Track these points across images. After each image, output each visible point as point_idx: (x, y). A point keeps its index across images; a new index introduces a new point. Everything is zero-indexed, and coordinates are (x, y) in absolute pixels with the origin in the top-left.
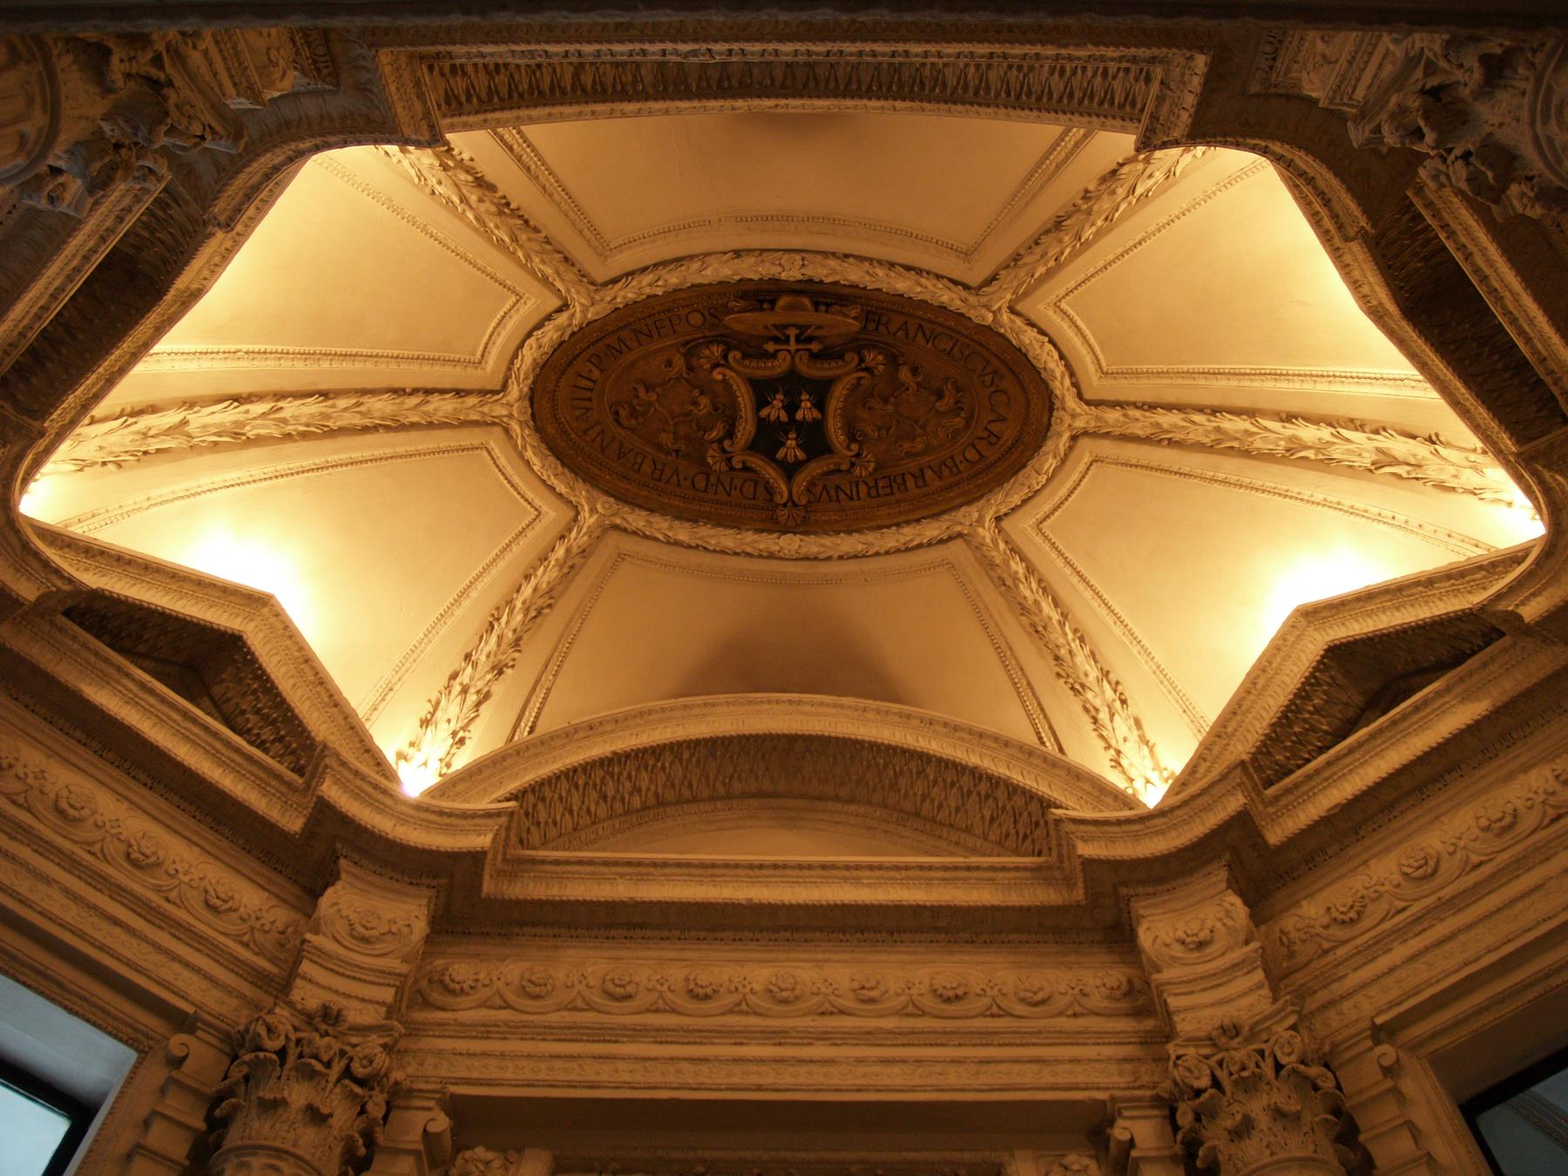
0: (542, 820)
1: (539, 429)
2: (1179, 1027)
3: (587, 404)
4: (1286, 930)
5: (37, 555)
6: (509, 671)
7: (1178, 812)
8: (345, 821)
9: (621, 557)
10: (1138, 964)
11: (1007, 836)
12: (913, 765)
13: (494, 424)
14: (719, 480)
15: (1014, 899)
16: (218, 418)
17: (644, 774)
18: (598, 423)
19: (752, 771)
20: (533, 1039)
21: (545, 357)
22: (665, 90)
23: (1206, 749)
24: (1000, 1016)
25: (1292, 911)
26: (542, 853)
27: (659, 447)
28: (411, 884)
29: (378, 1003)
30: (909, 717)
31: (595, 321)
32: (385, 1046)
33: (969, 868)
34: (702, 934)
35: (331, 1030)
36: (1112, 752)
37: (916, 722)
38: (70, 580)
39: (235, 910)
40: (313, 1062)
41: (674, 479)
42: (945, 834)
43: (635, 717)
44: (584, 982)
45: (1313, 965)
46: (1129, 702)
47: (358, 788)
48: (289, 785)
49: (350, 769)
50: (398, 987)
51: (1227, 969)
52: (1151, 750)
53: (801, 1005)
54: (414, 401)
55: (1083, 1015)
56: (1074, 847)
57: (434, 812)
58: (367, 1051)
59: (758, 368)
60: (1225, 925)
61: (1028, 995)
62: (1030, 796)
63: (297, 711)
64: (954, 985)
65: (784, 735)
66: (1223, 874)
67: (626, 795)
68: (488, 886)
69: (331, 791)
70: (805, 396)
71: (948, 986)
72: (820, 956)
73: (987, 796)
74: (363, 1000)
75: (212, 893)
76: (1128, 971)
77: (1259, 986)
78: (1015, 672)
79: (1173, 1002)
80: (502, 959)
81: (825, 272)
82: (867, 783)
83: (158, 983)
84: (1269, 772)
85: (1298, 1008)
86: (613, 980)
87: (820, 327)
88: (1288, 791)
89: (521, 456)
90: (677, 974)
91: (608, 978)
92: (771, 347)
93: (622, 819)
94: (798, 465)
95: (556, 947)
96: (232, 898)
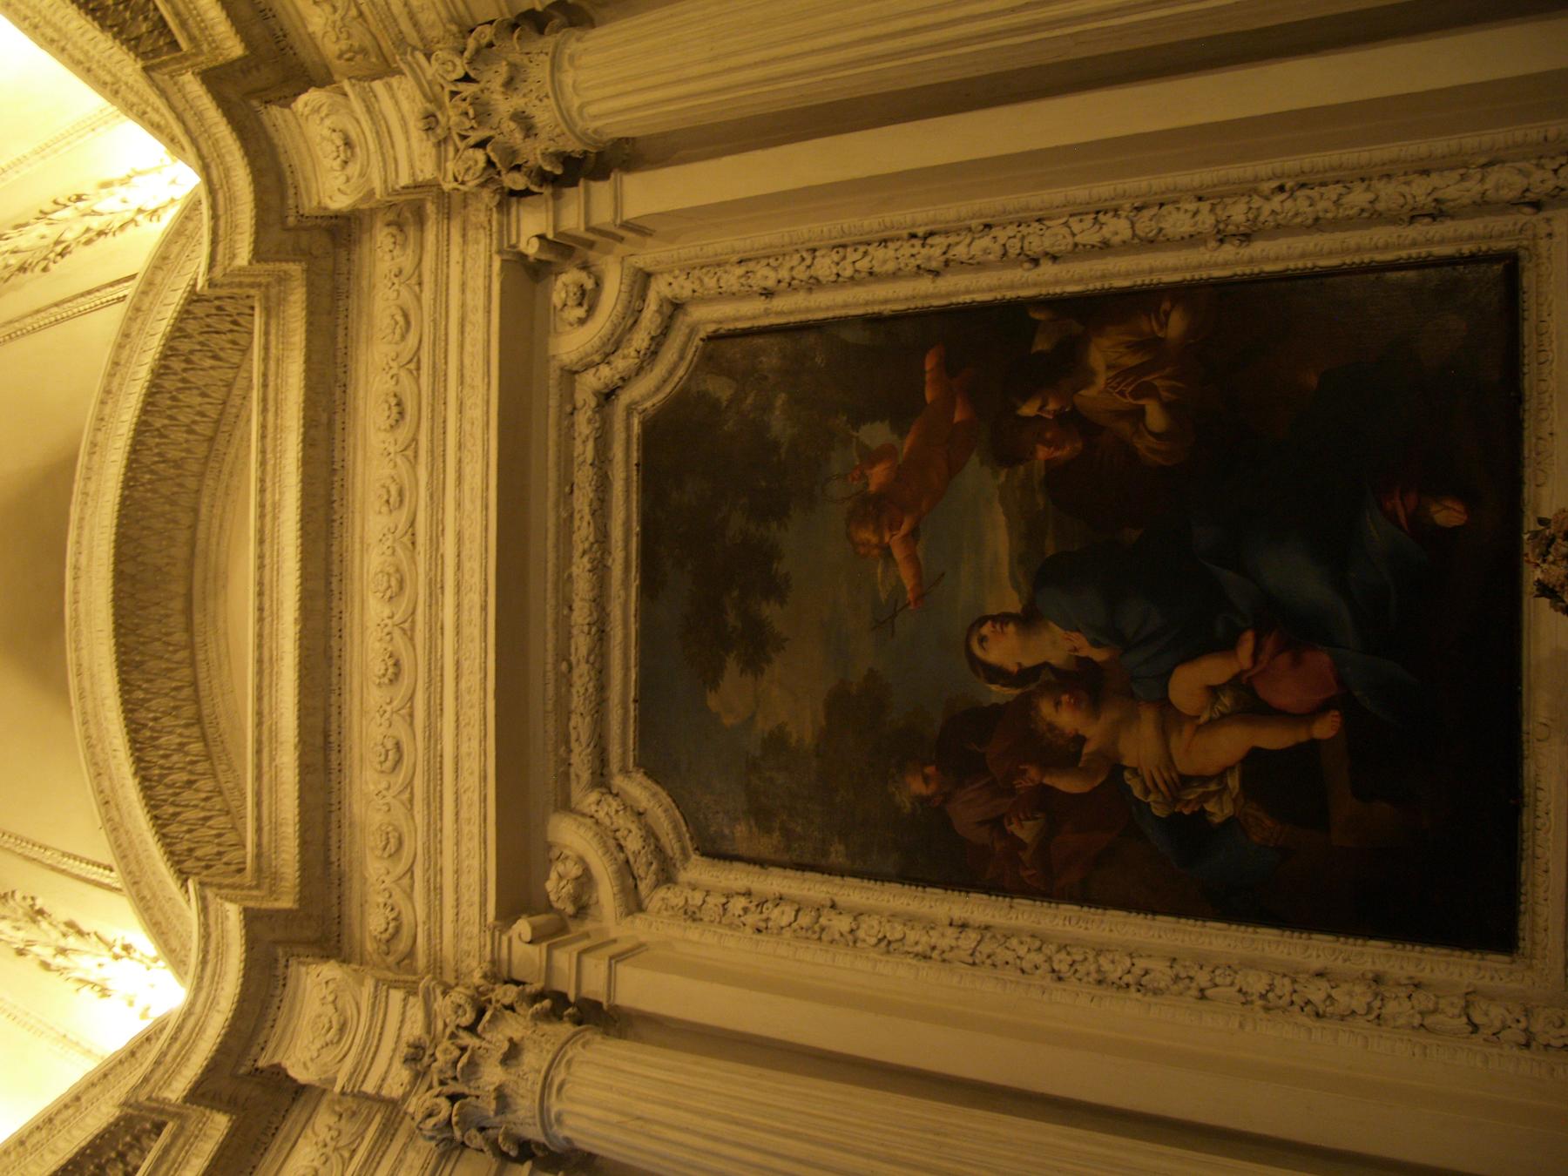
0: (216, 850)
2: (429, 176)
4: (337, 52)
6: (39, 904)
7: (205, 150)
8: (213, 1068)
10: (373, 212)
11: (234, 342)
12: (152, 441)
15: (298, 338)
17: (162, 740)
19: (160, 621)
20: (441, 842)
23: (131, 109)
24: (419, 361)
25: (319, 41)
28: (284, 985)
29: (405, 1006)
30: (94, 444)
32: (445, 993)
33: (265, 385)
34: (335, 671)
35: (429, 1052)
36: (140, 218)
37: (100, 437)
40: (460, 1065)
42: (234, 410)
43: (93, 754)
44: (384, 793)
45: (373, 29)
46: (79, 192)
47: (174, 1059)
48: (175, 1137)
49: (152, 1071)
50: (389, 988)
51: (372, 119)
52: (139, 174)
53: (405, 566)
55: (420, 276)
56: (241, 269)
57: (203, 970)
58: (449, 1012)
60: (327, 115)
61: (398, 331)
62: (185, 314)
63: (84, 1144)
64: (386, 406)
65: (115, 585)
66: (275, 110)
67: (188, 759)
68: (287, 902)
69: (176, 1090)
71: (387, 413)
72: (357, 546)
73: (188, 361)
74: (402, 1022)
76: (379, 225)
77: (389, 87)
78: (42, 319)
79: (405, 180)
80: (364, 880)
82: (173, 494)
84: (161, 43)
85: (409, 49)
86: (381, 763)
88: (183, 24)
90: (375, 696)
91: (378, 767)
93: (216, 763)
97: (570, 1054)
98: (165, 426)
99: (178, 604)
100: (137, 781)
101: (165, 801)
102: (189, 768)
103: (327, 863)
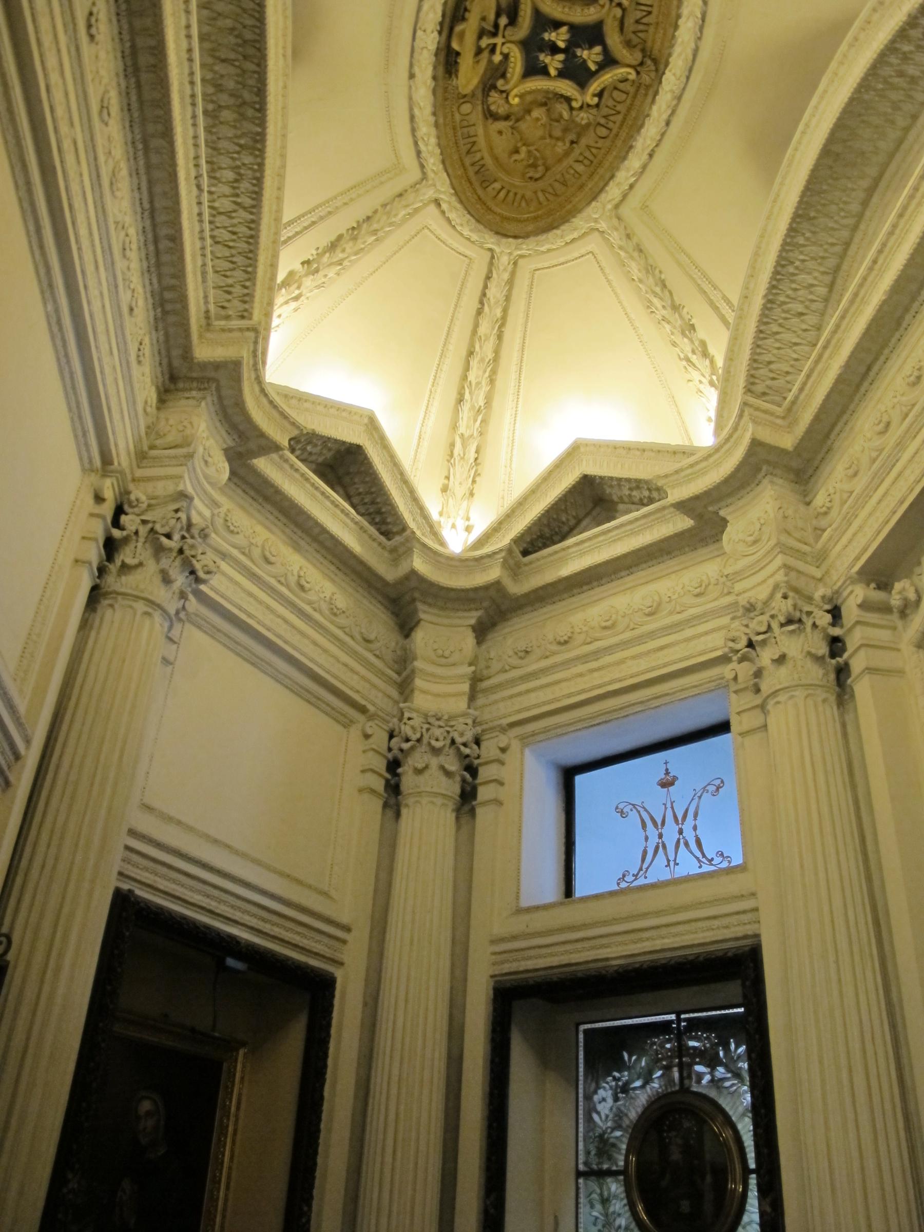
1: (526, 236)
3: (519, 196)
5: (482, 558)
8: (696, 498)
9: (645, 207)
13: (515, 264)
14: (605, 117)
16: (465, 419)
18: (535, 192)
21: (473, 221)
22: (259, 150)
26: (790, 397)
27: (567, 154)
30: (856, 39)
31: (452, 184)
34: (897, 335)
35: (756, 613)
38: (501, 550)
39: (709, 584)
41: (594, 151)
47: (685, 477)
54: (486, 308)
57: (725, 443)
59: (514, 68)
69: (676, 494)
70: (546, 36)
75: (691, 589)
81: (431, 15)
83: (700, 655)
87: (484, 19)
89: (543, 252)
92: (497, 58)
94: (606, 51)
95: (852, 428)
96: (702, 581)
97: (797, 693)
98: (911, 52)
99: (865, 183)
100: (763, 302)
101: (776, 320)
102: (807, 303)
103: (827, 436)
